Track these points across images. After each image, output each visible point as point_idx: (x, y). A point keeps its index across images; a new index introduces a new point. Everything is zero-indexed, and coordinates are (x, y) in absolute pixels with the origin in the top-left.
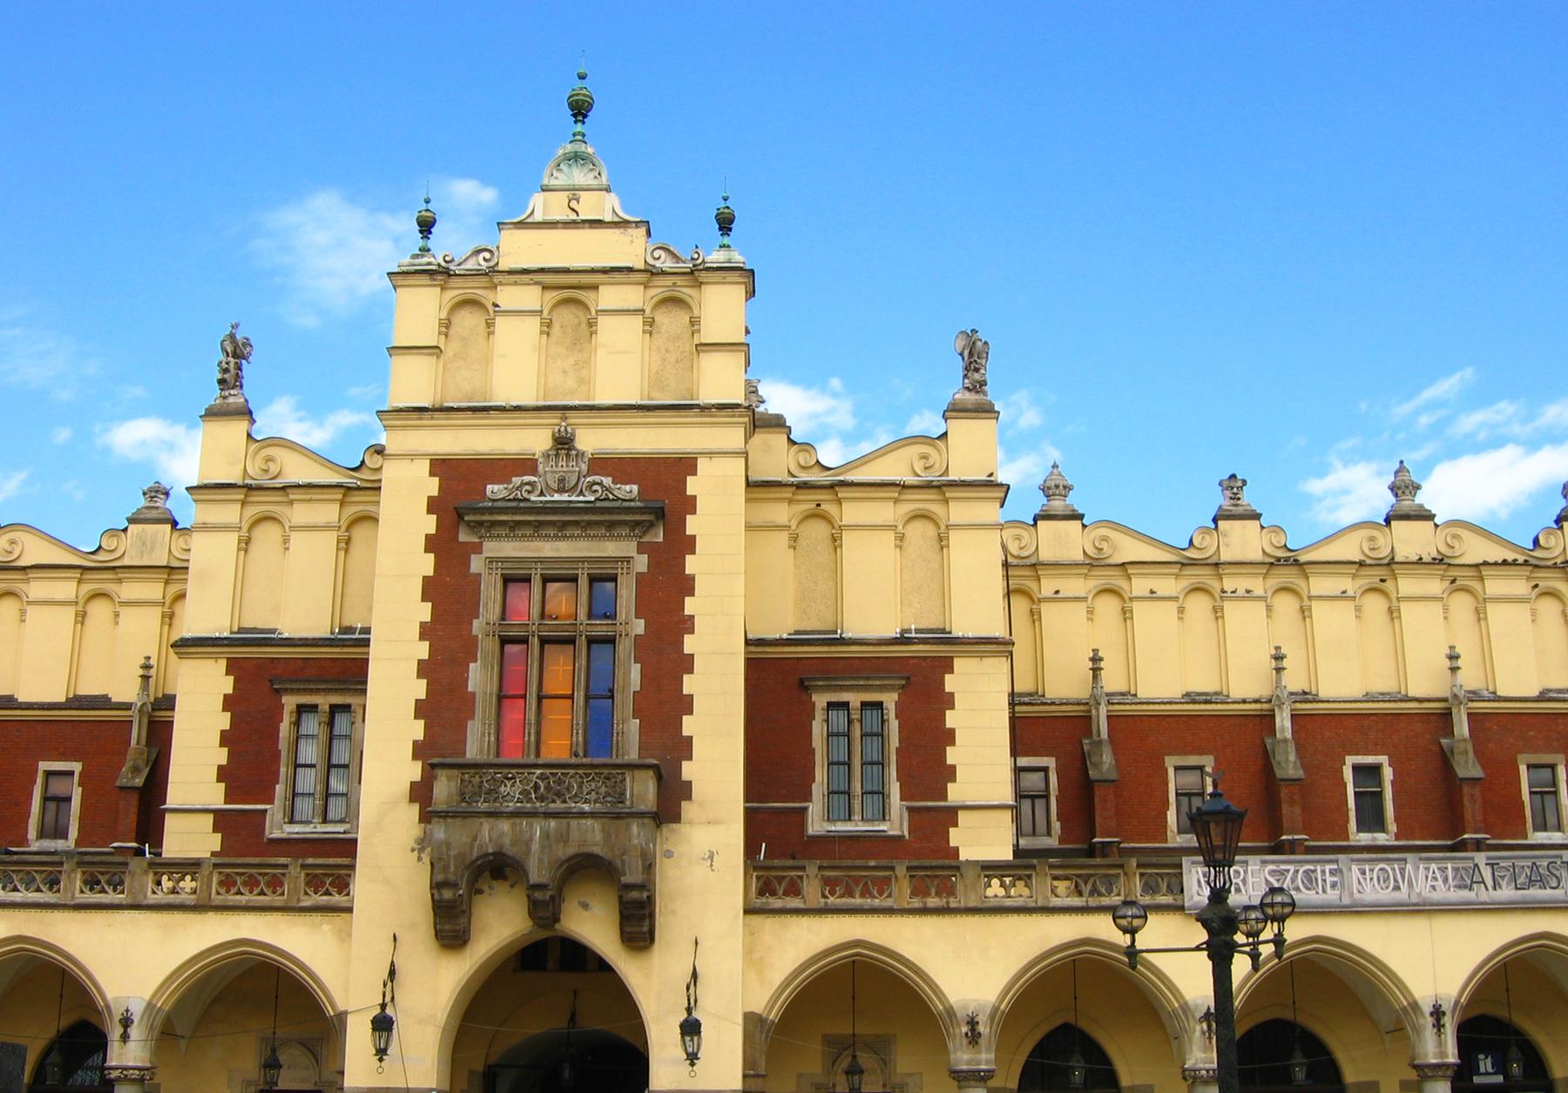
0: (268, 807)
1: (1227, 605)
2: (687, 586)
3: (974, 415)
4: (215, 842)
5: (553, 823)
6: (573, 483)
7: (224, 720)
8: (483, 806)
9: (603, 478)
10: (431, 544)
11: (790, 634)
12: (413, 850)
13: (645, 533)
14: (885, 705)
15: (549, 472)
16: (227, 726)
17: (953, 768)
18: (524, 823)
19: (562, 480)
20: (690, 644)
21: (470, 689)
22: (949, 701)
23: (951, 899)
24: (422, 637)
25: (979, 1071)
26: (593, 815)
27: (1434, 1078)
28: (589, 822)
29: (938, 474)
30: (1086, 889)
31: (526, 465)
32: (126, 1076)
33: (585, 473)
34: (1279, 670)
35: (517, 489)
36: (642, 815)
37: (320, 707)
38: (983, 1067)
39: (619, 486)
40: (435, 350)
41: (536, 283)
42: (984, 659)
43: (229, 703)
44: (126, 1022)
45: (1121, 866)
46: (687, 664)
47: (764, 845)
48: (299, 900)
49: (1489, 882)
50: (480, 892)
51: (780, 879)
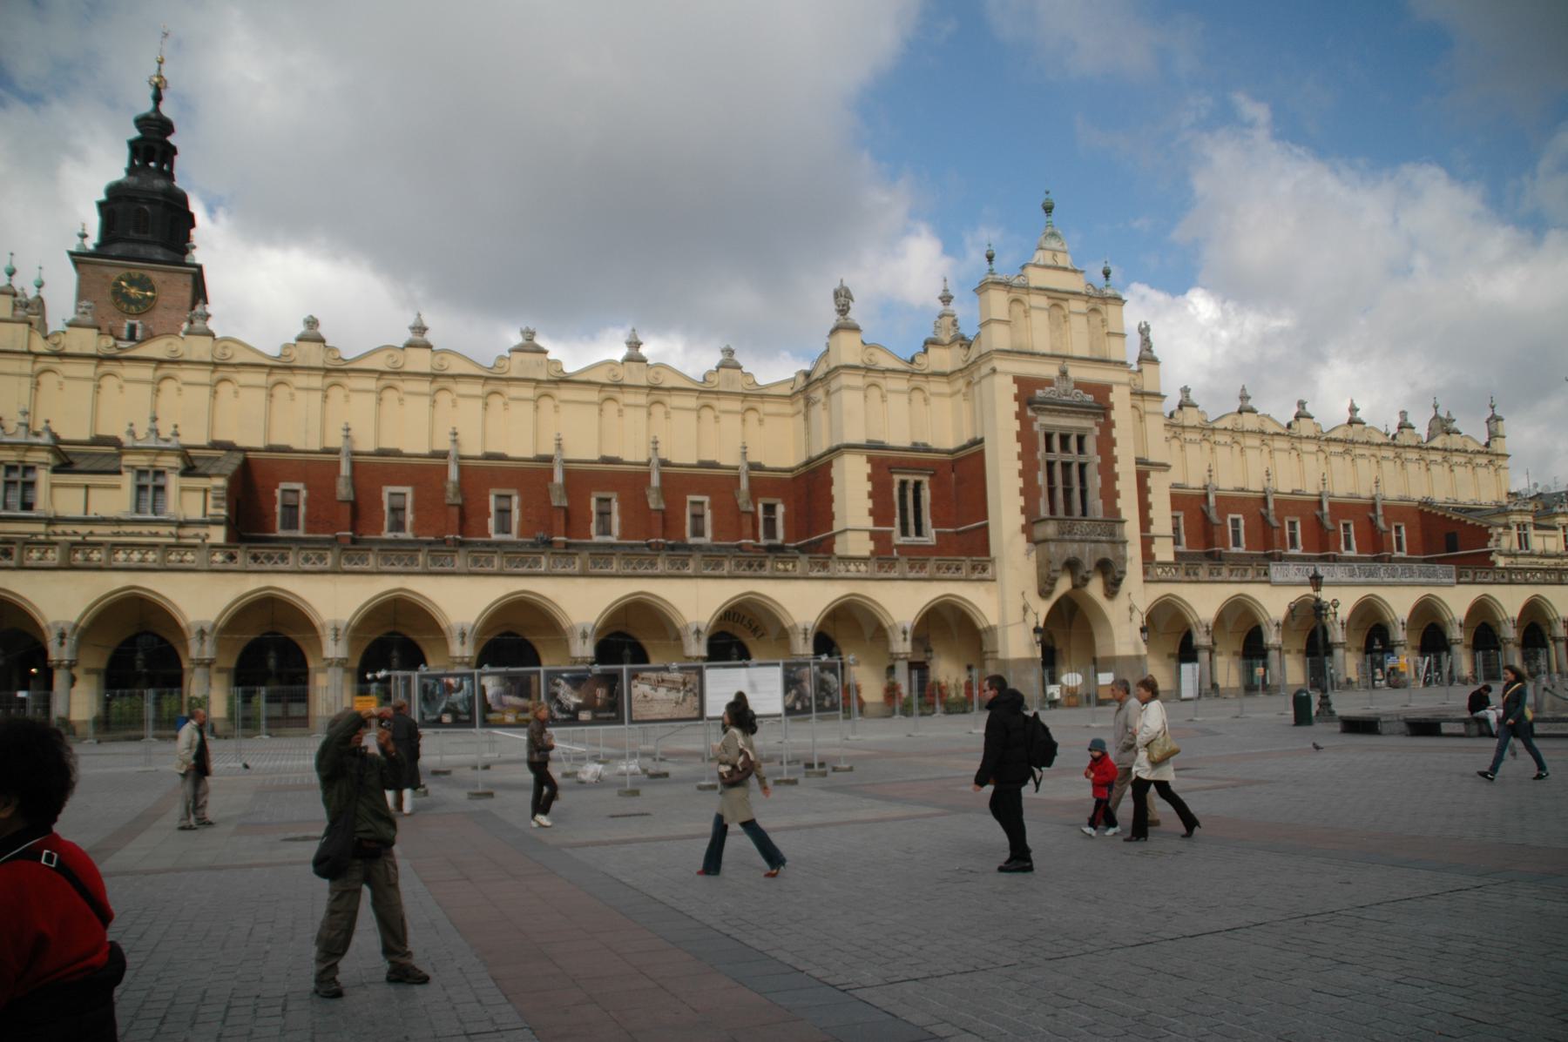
2: (1113, 443)
4: (871, 546)
5: (1093, 545)
19: (1066, 390)
26: (1107, 542)
27: (1339, 647)
28: (1105, 545)
30: (1215, 571)
40: (1007, 322)
43: (870, 478)
45: (1251, 565)
46: (1115, 477)
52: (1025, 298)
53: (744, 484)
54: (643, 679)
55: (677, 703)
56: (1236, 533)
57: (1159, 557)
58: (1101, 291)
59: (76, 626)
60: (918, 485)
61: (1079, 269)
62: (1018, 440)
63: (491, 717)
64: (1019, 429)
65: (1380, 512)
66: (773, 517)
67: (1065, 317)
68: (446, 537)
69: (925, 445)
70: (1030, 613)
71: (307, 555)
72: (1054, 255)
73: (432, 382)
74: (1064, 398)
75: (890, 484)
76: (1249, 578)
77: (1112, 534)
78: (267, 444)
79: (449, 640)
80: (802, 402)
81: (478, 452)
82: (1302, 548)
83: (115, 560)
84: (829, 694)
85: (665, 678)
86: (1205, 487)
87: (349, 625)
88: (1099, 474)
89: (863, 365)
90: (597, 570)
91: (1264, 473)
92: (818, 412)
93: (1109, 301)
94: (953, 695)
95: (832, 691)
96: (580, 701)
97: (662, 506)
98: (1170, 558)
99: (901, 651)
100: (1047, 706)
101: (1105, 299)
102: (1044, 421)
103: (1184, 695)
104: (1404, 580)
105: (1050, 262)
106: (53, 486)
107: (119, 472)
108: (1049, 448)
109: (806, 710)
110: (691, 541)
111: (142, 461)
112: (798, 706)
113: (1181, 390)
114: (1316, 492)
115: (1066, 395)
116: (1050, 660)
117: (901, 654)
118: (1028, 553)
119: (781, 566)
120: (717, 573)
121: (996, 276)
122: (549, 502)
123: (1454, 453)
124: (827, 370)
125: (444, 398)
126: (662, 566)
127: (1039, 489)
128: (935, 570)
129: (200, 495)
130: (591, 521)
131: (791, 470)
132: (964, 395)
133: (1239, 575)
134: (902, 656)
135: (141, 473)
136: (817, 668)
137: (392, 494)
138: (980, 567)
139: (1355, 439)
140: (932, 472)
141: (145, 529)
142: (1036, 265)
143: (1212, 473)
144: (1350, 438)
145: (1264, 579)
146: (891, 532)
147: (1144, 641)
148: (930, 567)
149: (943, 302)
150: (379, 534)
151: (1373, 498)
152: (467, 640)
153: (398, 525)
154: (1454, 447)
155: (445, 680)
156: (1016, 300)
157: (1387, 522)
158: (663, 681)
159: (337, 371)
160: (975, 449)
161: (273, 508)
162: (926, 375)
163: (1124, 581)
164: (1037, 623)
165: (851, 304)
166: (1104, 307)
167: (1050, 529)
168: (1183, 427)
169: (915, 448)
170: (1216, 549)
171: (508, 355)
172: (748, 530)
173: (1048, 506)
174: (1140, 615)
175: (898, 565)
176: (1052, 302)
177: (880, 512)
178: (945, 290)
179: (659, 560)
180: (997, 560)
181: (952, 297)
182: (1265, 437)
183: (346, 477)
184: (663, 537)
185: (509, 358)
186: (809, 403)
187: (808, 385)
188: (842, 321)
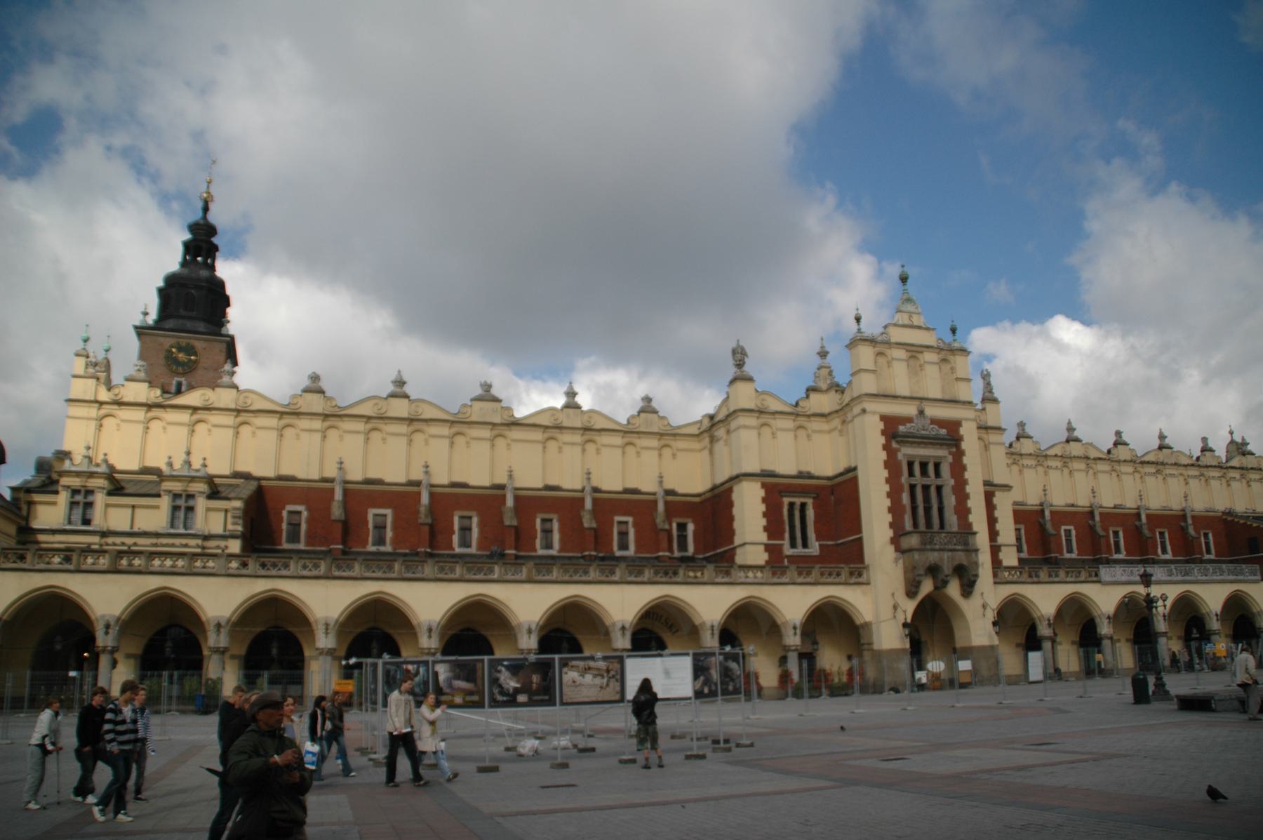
1: (1025, 470)
2: (964, 468)
5: (950, 553)
8: (929, 547)
19: (923, 426)
26: (962, 550)
27: (1163, 636)
28: (960, 553)
30: (1053, 574)
34: (1045, 495)
40: (874, 371)
43: (764, 500)
45: (1082, 568)
46: (967, 496)
49: (1175, 573)
52: (888, 352)
53: (661, 507)
54: (572, 667)
55: (601, 687)
56: (1069, 541)
57: (1006, 563)
58: (949, 344)
59: (119, 619)
60: (803, 506)
61: (931, 327)
63: (443, 698)
64: (886, 458)
65: (1190, 521)
66: (685, 534)
67: (921, 366)
68: (419, 550)
69: (809, 473)
70: (899, 609)
71: (305, 563)
72: (911, 316)
73: (408, 425)
74: (923, 432)
75: (780, 505)
76: (1082, 579)
77: (966, 544)
78: (276, 474)
79: (419, 635)
80: (707, 440)
81: (445, 481)
82: (1125, 553)
83: (152, 566)
84: (732, 680)
85: (591, 666)
86: (1041, 504)
87: (337, 621)
88: (954, 494)
89: (756, 409)
90: (540, 578)
91: (1091, 491)
92: (719, 447)
93: (957, 352)
94: (836, 680)
95: (735, 677)
96: (518, 685)
97: (594, 525)
98: (1015, 563)
99: (792, 644)
100: (916, 689)
101: (953, 351)
102: (905, 452)
103: (1032, 678)
104: (1215, 578)
105: (907, 322)
106: (107, 506)
107: (159, 496)
108: (911, 474)
109: (713, 694)
110: (618, 553)
111: (177, 487)
112: (706, 690)
113: (1018, 424)
114: (1135, 506)
115: (923, 430)
116: (917, 651)
117: (793, 646)
118: (896, 561)
119: (691, 574)
120: (639, 579)
121: (863, 334)
122: (501, 521)
123: (1250, 471)
124: (727, 413)
125: (418, 437)
126: (593, 574)
127: (904, 506)
128: (819, 576)
129: (222, 514)
130: (536, 538)
131: (699, 495)
132: (841, 431)
133: (1074, 577)
134: (793, 648)
135: (176, 496)
136: (721, 658)
137: (376, 515)
138: (857, 573)
139: (1165, 461)
140: (815, 495)
141: (177, 541)
142: (895, 325)
143: (1047, 492)
144: (1161, 460)
145: (1095, 579)
146: (782, 545)
147: (996, 633)
148: (815, 573)
149: (821, 356)
150: (365, 547)
151: (1183, 510)
152: (433, 634)
153: (380, 541)
154: (1250, 466)
155: (405, 666)
156: (880, 354)
157: (1196, 530)
158: (590, 668)
159: (334, 416)
160: (850, 475)
161: (281, 526)
162: (809, 416)
163: (978, 583)
164: (906, 619)
165: (746, 360)
166: (952, 357)
167: (914, 541)
168: (1021, 455)
169: (801, 475)
170: (1053, 555)
171: (469, 403)
172: (665, 544)
173: (912, 522)
174: (992, 612)
175: (788, 573)
176: (909, 354)
177: (773, 528)
178: (822, 347)
179: (591, 570)
180: (871, 568)
181: (827, 353)
182: (1089, 462)
183: (339, 501)
184: (596, 550)
185: (471, 406)
186: (713, 440)
187: (713, 426)
188: (739, 373)
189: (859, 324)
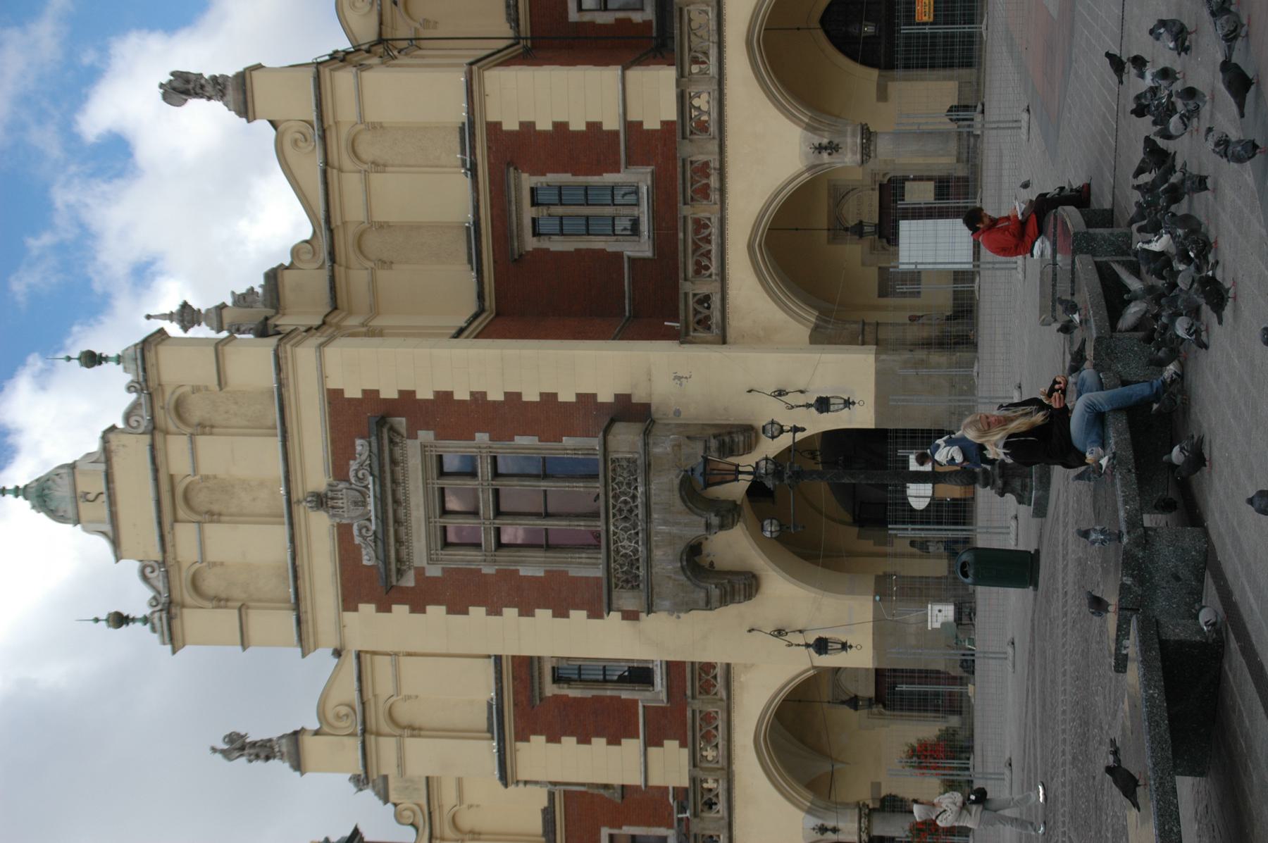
0: (640, 705)
2: (444, 398)
3: (249, 94)
4: (671, 745)
5: (655, 516)
6: (357, 494)
7: (569, 742)
8: (642, 572)
9: (351, 469)
10: (418, 608)
11: (472, 269)
12: (679, 617)
13: (399, 433)
14: (533, 186)
15: (350, 514)
16: (574, 739)
17: (589, 124)
18: (655, 538)
19: (356, 503)
20: (495, 395)
21: (539, 573)
22: (528, 127)
23: (712, 165)
24: (499, 613)
25: (862, 143)
26: (647, 483)
28: (653, 487)
29: (311, 130)
31: (343, 533)
32: (866, 828)
33: (347, 485)
35: (366, 540)
36: (646, 444)
37: (554, 665)
38: (859, 141)
39: (357, 456)
40: (240, 609)
41: (172, 528)
42: (486, 93)
43: (553, 738)
44: (823, 829)
46: (513, 398)
47: (666, 323)
48: (721, 700)
50: (712, 564)
51: (696, 312)
62: (465, 612)
176: (182, 513)
181: (185, 306)
189: (134, 620)
